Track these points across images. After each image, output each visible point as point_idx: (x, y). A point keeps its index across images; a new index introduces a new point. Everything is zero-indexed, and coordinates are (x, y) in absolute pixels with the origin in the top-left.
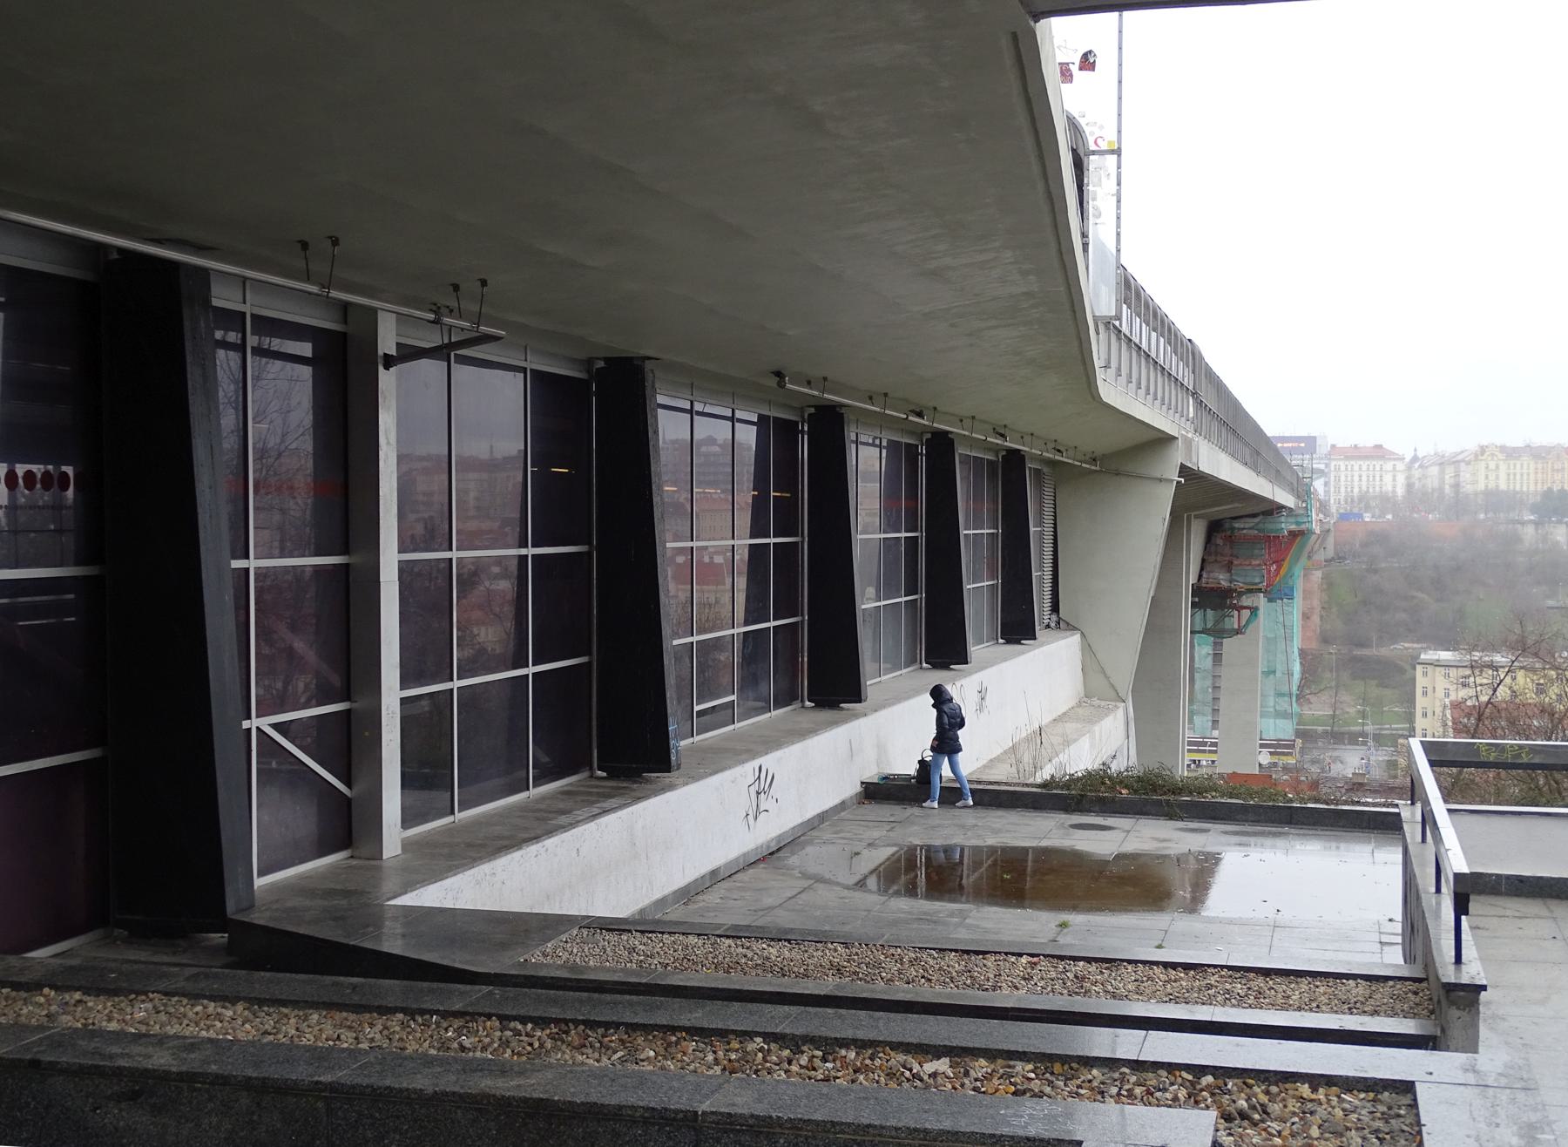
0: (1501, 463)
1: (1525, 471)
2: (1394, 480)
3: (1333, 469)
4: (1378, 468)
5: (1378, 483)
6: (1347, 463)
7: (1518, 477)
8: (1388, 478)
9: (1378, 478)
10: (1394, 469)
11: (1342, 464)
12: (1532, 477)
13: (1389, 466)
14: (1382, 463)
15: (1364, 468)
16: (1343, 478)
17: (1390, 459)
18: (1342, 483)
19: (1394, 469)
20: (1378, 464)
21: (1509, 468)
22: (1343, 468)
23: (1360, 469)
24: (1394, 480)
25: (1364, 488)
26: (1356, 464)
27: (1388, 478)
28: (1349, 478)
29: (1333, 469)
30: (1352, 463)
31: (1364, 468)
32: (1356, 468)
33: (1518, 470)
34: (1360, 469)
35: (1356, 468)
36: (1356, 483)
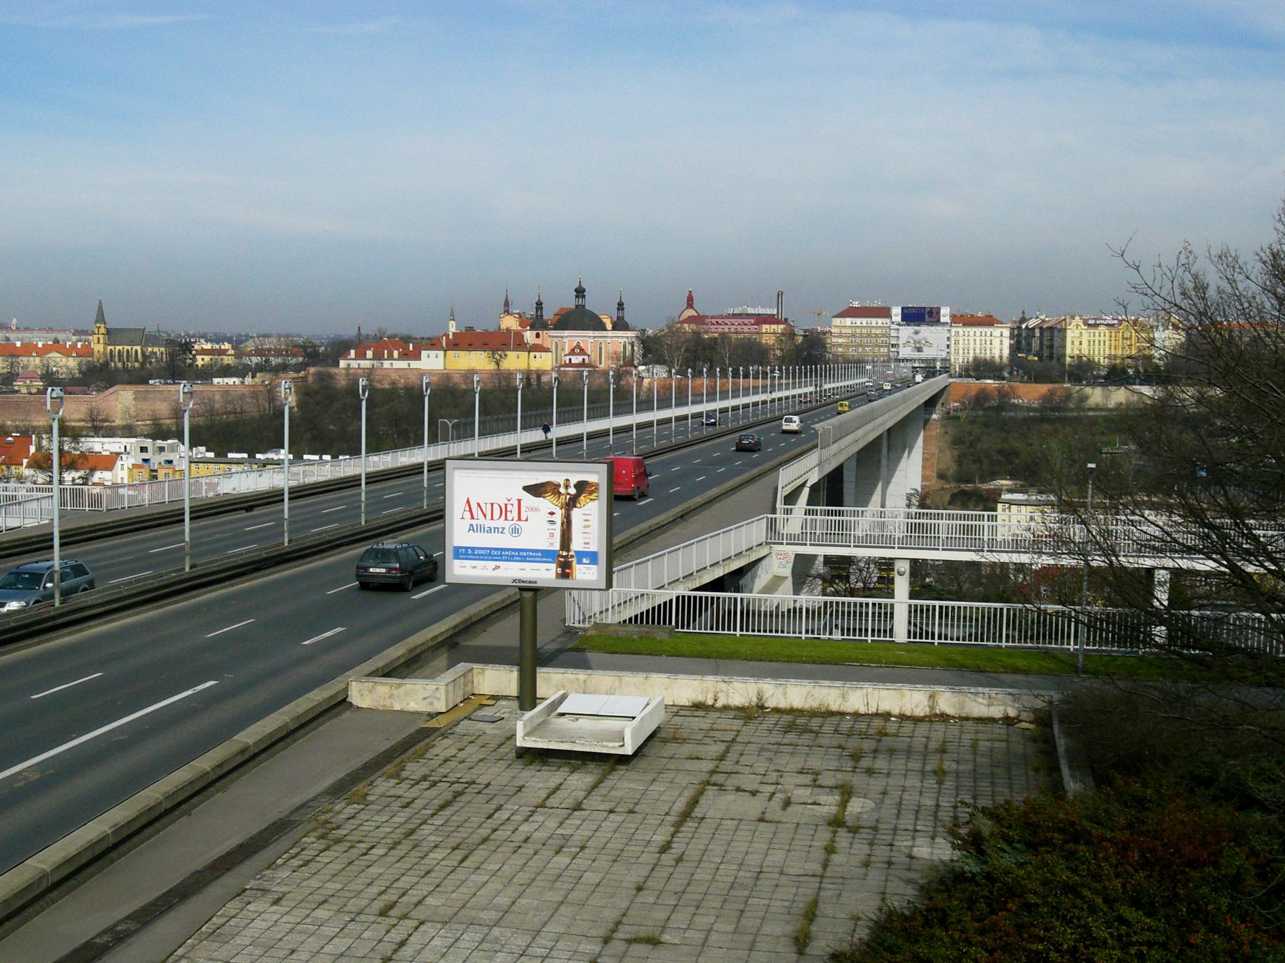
0: (1083, 331)
1: (1102, 338)
2: (1001, 344)
3: (953, 334)
4: (988, 334)
5: (988, 346)
6: (964, 329)
7: (1097, 343)
8: (996, 342)
9: (988, 343)
10: (1001, 335)
11: (960, 330)
12: (1107, 343)
13: (997, 332)
14: (991, 330)
15: (978, 334)
16: (961, 342)
17: (998, 327)
18: (961, 346)
19: (1001, 335)
20: (988, 330)
21: (1090, 336)
22: (961, 334)
23: (975, 335)
24: (1001, 344)
25: (978, 351)
26: (971, 330)
27: (996, 342)
28: (966, 342)
29: (953, 334)
30: (969, 329)
31: (978, 334)
32: (972, 334)
33: (1097, 338)
34: (975, 335)
35: (972, 334)
36: (972, 346)
